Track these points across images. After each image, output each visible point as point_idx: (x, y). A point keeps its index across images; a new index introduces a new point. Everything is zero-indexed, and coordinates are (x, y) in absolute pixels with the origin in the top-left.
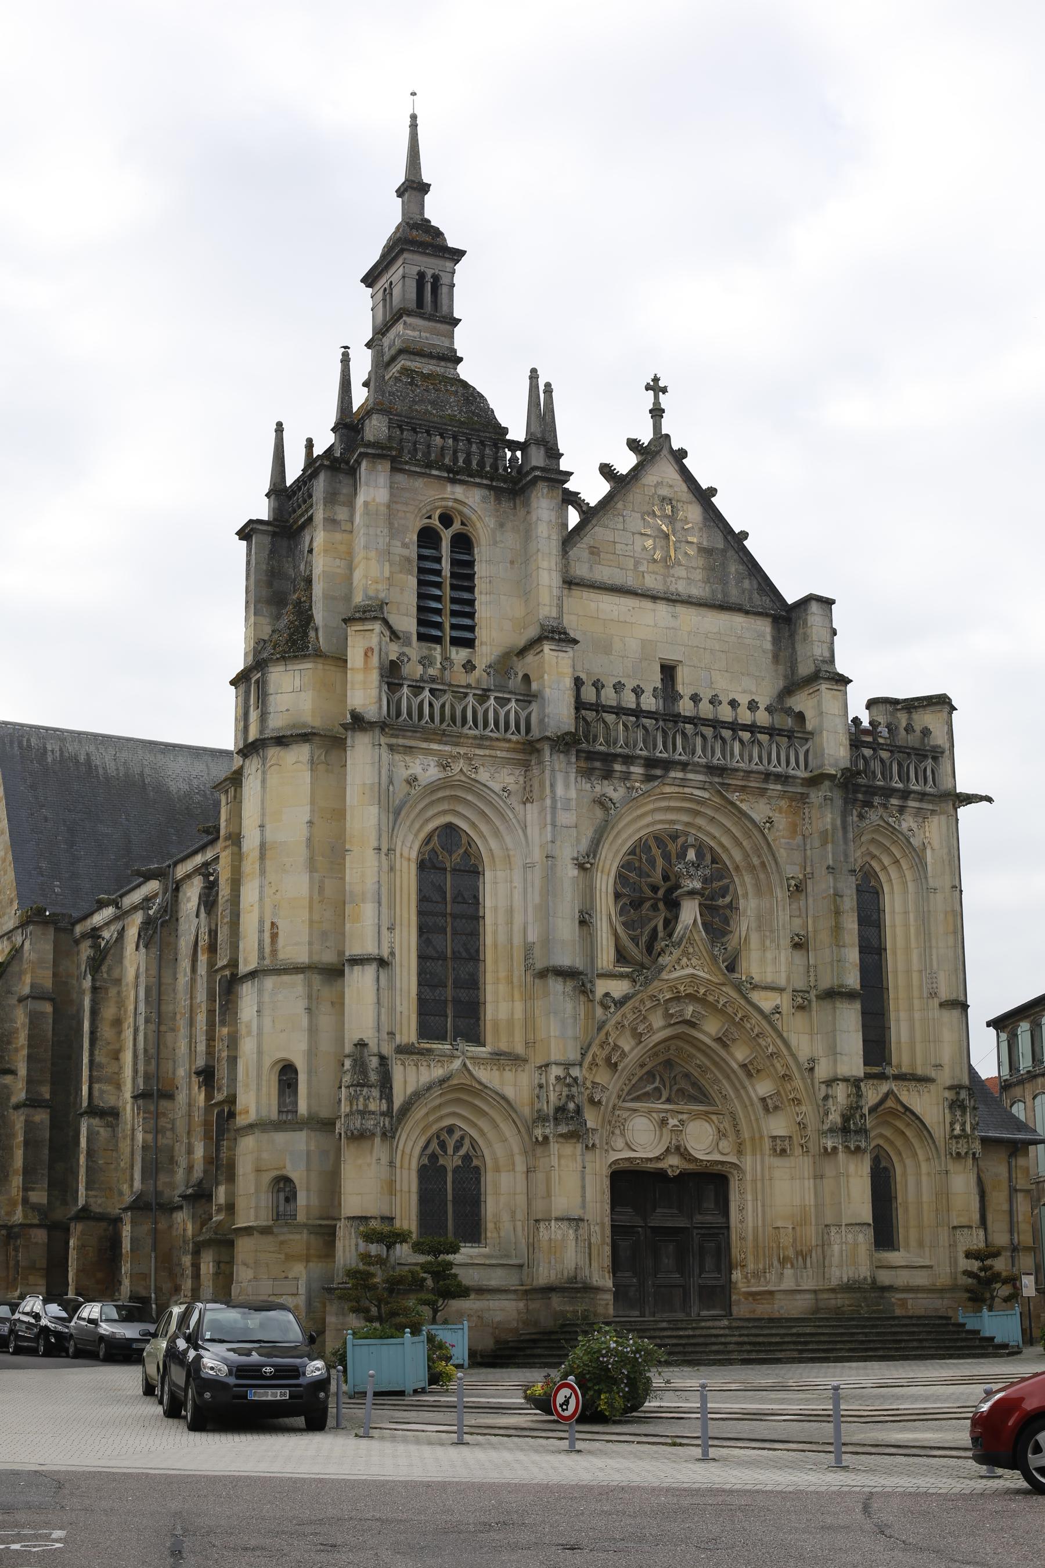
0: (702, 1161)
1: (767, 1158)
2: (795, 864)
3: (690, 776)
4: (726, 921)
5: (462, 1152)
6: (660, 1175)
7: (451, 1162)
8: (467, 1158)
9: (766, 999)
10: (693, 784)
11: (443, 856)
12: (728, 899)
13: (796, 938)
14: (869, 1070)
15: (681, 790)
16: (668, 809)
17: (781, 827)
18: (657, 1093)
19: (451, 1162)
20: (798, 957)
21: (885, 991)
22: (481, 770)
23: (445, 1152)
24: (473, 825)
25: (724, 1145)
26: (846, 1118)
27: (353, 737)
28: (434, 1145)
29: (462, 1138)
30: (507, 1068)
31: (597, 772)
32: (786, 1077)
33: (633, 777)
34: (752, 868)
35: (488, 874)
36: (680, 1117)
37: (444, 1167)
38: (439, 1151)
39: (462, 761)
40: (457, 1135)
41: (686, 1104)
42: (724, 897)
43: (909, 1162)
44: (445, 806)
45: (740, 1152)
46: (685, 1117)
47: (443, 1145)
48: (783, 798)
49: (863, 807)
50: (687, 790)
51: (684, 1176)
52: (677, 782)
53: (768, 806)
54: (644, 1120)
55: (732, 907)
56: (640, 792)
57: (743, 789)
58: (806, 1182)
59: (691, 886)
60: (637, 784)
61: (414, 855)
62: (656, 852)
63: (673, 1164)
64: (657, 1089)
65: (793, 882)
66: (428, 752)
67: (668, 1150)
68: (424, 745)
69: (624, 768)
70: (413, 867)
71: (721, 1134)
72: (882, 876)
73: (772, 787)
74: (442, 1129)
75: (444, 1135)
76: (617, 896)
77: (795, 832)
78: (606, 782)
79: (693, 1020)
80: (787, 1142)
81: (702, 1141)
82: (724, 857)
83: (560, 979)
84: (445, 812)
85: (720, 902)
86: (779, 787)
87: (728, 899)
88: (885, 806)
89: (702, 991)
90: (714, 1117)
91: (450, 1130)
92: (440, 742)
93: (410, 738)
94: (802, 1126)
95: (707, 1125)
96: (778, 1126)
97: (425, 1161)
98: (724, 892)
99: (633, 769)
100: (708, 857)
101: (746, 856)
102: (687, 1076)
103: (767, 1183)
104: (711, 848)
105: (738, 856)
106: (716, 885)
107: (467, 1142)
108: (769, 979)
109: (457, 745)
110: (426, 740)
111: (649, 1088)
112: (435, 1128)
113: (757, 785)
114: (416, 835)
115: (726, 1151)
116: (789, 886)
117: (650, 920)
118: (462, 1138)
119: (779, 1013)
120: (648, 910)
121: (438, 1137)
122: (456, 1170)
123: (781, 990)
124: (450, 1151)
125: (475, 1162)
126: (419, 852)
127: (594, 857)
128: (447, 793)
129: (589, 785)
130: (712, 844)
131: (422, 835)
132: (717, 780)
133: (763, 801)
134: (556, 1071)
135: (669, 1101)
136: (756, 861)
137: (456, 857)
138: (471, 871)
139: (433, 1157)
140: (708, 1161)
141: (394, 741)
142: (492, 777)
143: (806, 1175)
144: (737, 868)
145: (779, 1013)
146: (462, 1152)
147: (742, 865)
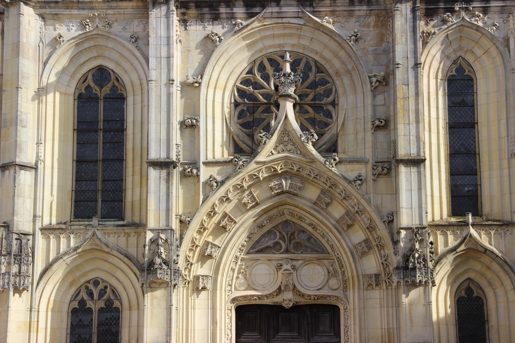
0: (309, 296)
1: (361, 291)
2: (382, 65)
3: (284, 9)
4: (329, 115)
5: (106, 297)
6: (277, 308)
7: (95, 306)
8: (109, 303)
9: (352, 170)
10: (289, 15)
11: (96, 89)
12: (331, 98)
13: (377, 122)
14: (453, 220)
15: (280, 21)
16: (274, 36)
17: (369, 38)
18: (275, 247)
19: (95, 306)
20: (381, 135)
21: (477, 156)
22: (115, 25)
23: (92, 298)
24: (118, 64)
25: (334, 282)
26: (406, 258)
27: (8, 11)
28: (84, 295)
29: (106, 287)
30: (111, 235)
31: (207, 16)
32: (371, 228)
33: (237, 15)
34: (348, 71)
35: (130, 100)
36: (294, 263)
37: (90, 311)
38: (86, 297)
39: (97, 20)
40: (101, 286)
41: (302, 253)
42: (328, 97)
43: (500, 291)
44: (94, 53)
45: (345, 289)
46: (297, 264)
47: (91, 294)
48: (370, 16)
49: (445, 13)
50: (285, 20)
51: (296, 308)
52: (275, 15)
53: (358, 24)
54: (265, 267)
55: (334, 104)
56: (241, 26)
57: (333, 13)
58: (390, 309)
59: (283, 90)
60: (239, 21)
61: (72, 90)
62: (270, 70)
63: (287, 299)
64: (276, 243)
65: (374, 80)
66: (71, 17)
67: (280, 288)
68: (67, 12)
69: (228, 10)
70: (71, 98)
71: (331, 274)
72: (476, 66)
73: (357, 8)
74: (88, 282)
75: (91, 286)
76: (237, 105)
77: (382, 40)
78: (216, 22)
79: (291, 190)
80: (373, 279)
81: (312, 281)
82: (327, 66)
83: (157, 168)
84: (95, 57)
85: (325, 100)
86: (365, 8)
87: (331, 98)
88: (466, 9)
89: (295, 169)
90: (326, 262)
91: (96, 283)
92: (79, 9)
93: (55, 8)
94: (385, 265)
95: (319, 268)
96: (371, 264)
97: (75, 304)
98: (328, 93)
99: (235, 10)
100: (314, 68)
101: (343, 63)
102: (304, 231)
103: (362, 311)
104: (316, 62)
105: (337, 63)
106: (320, 89)
107: (108, 290)
108: (359, 155)
109: (92, 9)
110: (67, 8)
111: (270, 243)
112: (83, 280)
113: (345, 8)
114: (72, 77)
115: (336, 287)
116: (371, 83)
117: (264, 120)
118: (106, 287)
119: (361, 180)
120: (263, 112)
121: (87, 288)
122: (101, 310)
123: (366, 162)
124: (96, 297)
125: (117, 304)
126: (76, 88)
127: (201, 78)
128: (92, 43)
129: (201, 27)
130: (317, 58)
131: (79, 76)
132: (308, 9)
133: (354, 20)
134: (150, 235)
135: (287, 251)
136: (350, 66)
137: (107, 90)
138: (118, 99)
139: (82, 302)
140: (316, 296)
141: (43, 11)
142: (124, 29)
143: (390, 305)
144: (337, 73)
145: (361, 180)
146: (79, 298)
147: (341, 71)
